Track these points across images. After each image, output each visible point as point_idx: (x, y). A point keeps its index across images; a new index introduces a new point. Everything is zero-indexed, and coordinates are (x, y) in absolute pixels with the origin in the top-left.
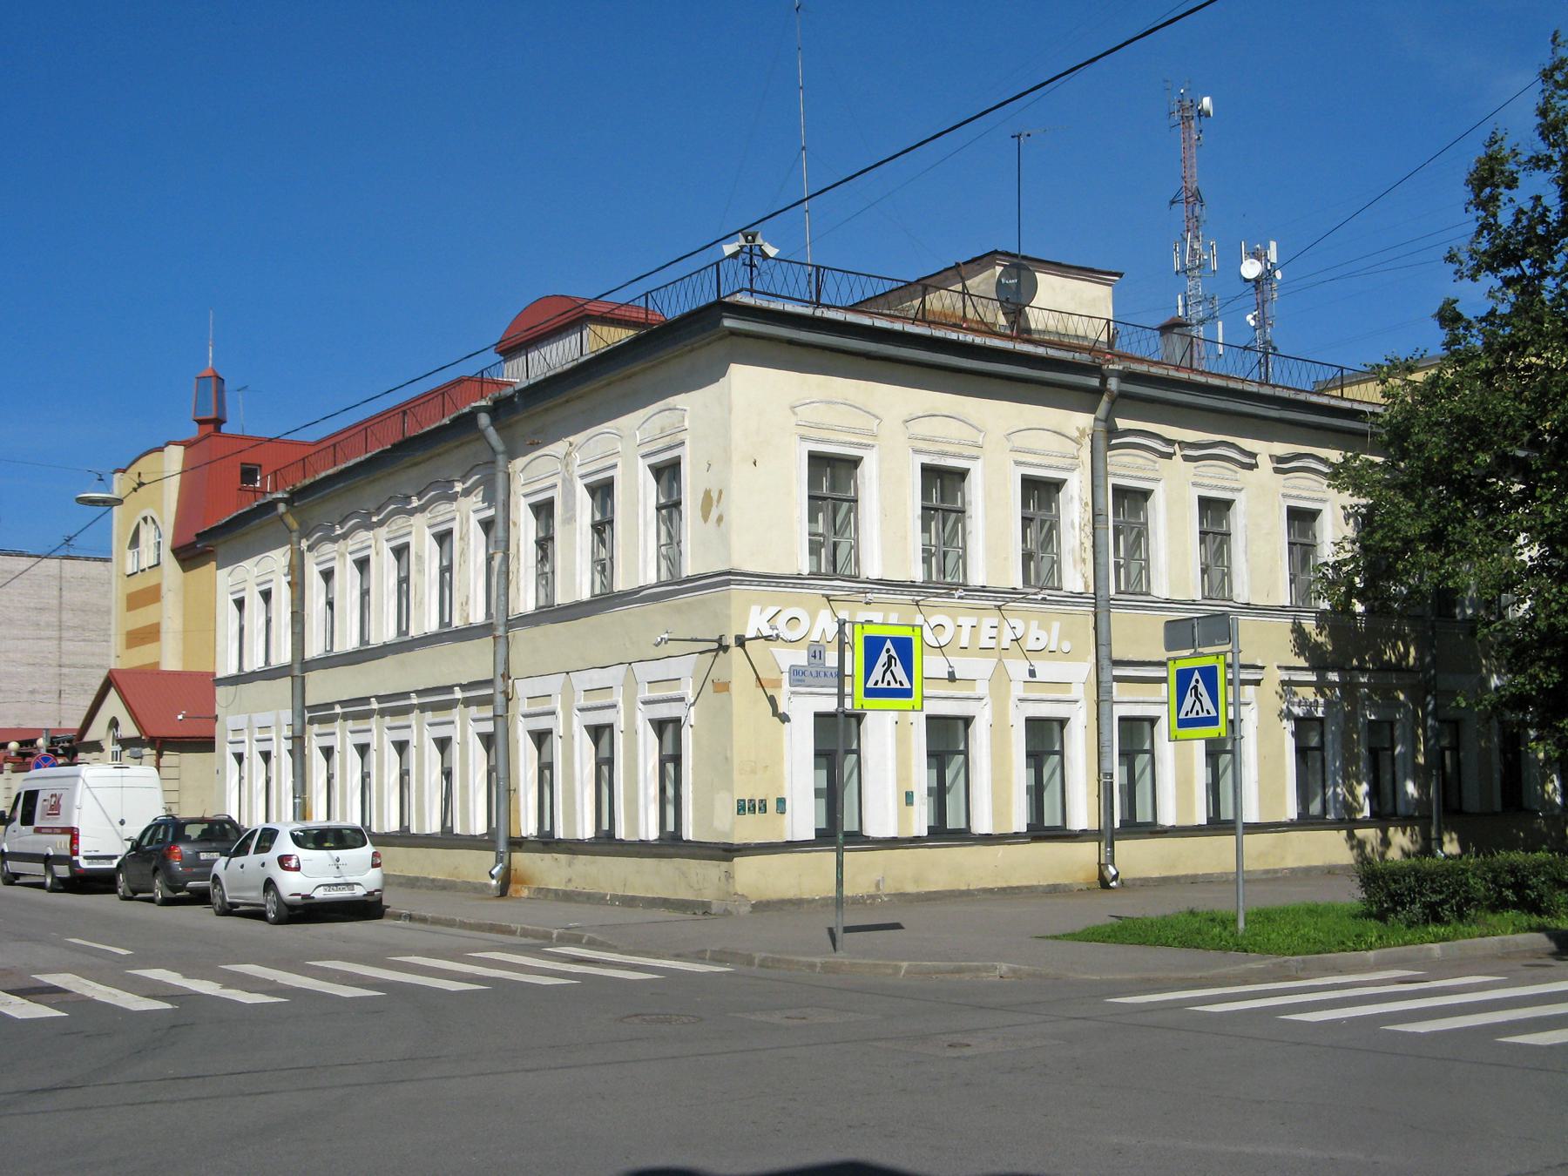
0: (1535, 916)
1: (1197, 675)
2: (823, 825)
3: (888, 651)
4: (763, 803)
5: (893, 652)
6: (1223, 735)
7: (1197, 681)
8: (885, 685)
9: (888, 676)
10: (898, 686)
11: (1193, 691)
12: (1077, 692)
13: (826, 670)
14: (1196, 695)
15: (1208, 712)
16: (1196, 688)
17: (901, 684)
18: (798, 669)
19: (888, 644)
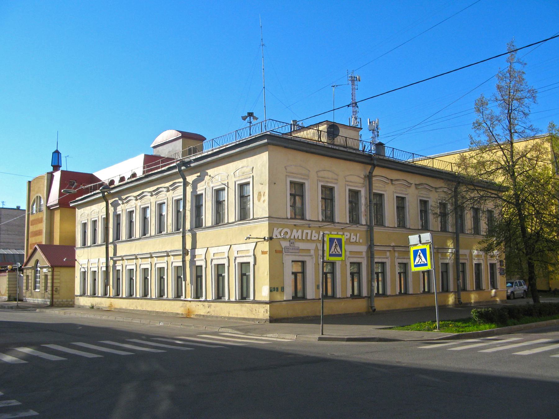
0: (512, 319)
1: (420, 251)
2: (294, 295)
3: (335, 242)
4: (277, 288)
5: (337, 243)
6: (430, 268)
7: (420, 253)
8: (335, 253)
9: (336, 250)
10: (338, 253)
11: (419, 256)
12: (364, 254)
13: (295, 248)
14: (420, 257)
15: (424, 262)
16: (419, 255)
17: (339, 253)
18: (287, 247)
19: (336, 241)
